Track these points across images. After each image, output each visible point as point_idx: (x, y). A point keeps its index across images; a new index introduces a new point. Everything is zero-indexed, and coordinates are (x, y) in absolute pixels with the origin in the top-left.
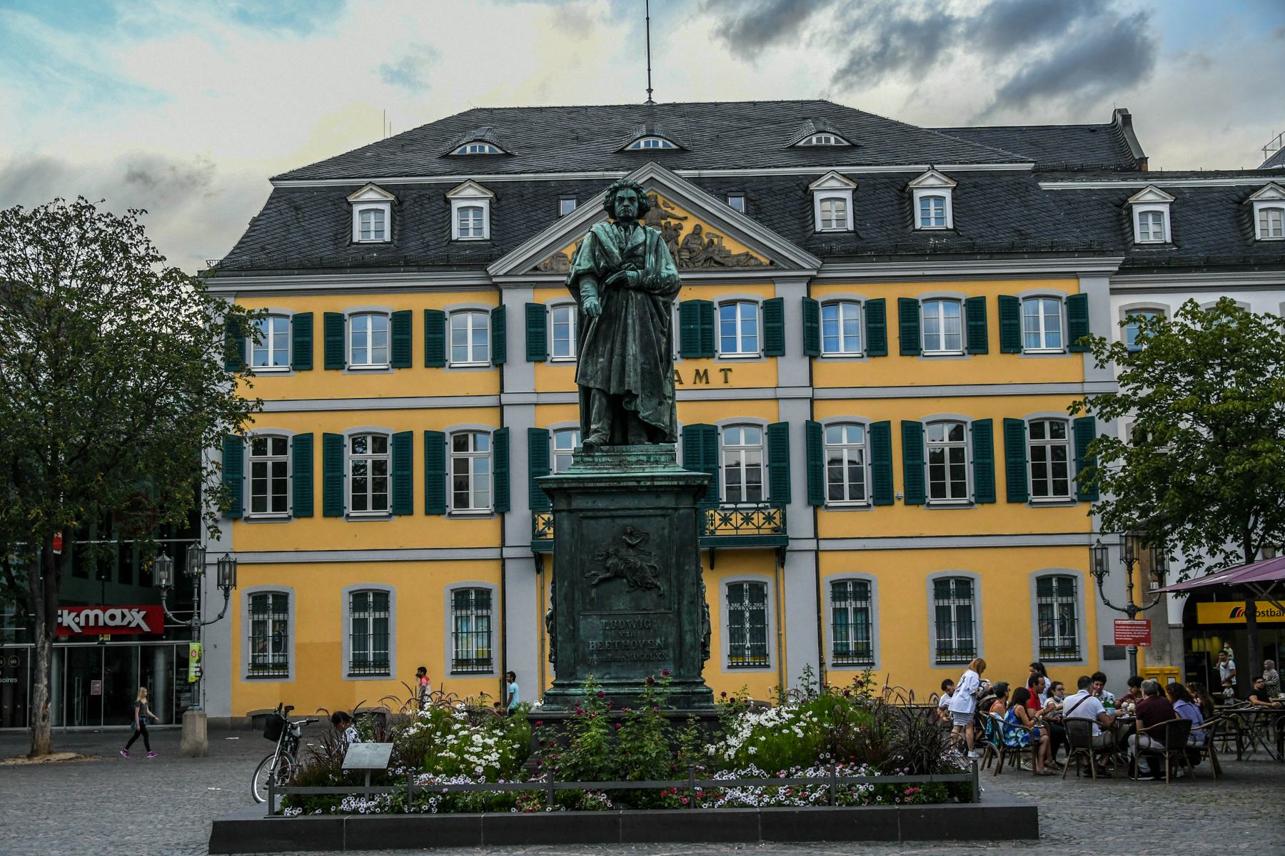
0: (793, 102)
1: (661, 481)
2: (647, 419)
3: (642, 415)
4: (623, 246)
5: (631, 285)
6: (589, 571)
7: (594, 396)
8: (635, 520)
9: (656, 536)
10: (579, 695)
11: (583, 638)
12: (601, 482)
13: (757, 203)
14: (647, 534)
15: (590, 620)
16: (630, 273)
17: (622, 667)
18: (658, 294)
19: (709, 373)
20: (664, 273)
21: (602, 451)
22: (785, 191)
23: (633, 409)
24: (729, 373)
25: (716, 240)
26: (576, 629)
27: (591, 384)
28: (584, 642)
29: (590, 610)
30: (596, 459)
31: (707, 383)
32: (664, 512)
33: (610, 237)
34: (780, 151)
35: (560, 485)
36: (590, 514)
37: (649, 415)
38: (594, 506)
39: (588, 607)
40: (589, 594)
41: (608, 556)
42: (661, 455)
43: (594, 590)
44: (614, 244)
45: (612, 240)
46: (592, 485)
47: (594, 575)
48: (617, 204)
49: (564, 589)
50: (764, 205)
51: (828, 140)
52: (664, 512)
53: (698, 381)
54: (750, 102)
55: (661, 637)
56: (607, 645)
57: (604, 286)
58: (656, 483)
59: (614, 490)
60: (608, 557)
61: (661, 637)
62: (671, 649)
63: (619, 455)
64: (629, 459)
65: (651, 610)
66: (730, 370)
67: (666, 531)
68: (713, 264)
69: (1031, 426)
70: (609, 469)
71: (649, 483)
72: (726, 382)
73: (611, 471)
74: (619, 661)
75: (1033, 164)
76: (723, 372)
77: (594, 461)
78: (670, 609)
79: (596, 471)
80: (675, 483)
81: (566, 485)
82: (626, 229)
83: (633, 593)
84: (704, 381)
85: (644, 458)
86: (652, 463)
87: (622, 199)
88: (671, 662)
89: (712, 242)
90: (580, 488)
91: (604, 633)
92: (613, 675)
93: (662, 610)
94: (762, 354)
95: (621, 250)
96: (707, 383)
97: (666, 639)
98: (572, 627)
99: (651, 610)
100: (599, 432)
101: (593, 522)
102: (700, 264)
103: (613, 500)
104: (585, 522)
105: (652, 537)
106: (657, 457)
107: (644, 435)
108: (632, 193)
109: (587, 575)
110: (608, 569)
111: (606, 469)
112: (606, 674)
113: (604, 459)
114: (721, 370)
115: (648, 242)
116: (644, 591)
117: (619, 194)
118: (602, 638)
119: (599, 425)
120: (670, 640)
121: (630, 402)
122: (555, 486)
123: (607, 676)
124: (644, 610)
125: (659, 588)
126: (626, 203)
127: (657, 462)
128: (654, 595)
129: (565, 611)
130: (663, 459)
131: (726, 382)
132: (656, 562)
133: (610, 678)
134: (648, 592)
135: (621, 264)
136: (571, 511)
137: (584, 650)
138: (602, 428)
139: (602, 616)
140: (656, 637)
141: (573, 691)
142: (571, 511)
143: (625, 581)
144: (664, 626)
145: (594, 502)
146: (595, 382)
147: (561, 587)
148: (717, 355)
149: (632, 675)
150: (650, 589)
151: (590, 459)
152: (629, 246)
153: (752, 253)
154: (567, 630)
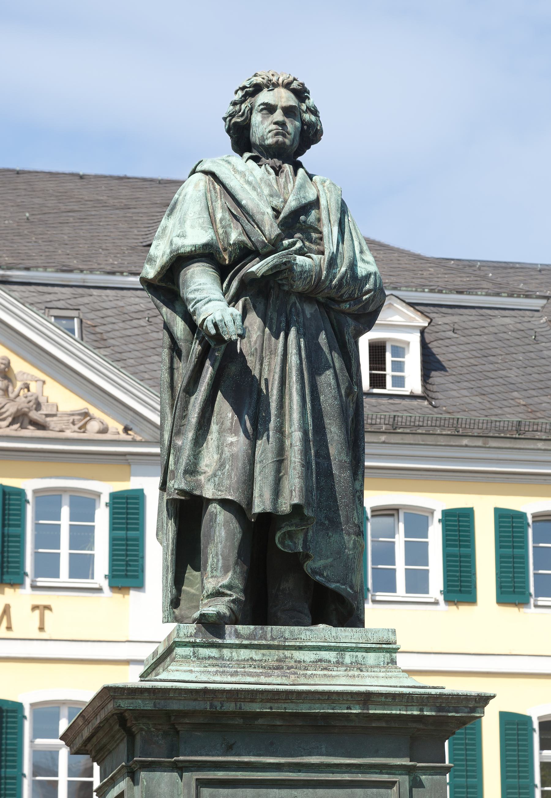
0: (145, 180)
2: (321, 575)
3: (309, 566)
4: (277, 202)
5: (299, 286)
7: (214, 517)
12: (253, 701)
13: (98, 330)
16: (300, 259)
18: (343, 312)
19: (13, 611)
20: (362, 270)
21: (238, 635)
22: (145, 314)
24: (47, 612)
25: (34, 387)
27: (208, 492)
30: (226, 652)
31: (9, 628)
33: (249, 183)
34: (133, 248)
35: (162, 704)
36: (221, 775)
37: (325, 567)
42: (367, 650)
44: (260, 195)
45: (254, 189)
46: (230, 707)
48: (256, 118)
50: (110, 335)
54: (73, 175)
57: (235, 284)
59: (278, 723)
63: (278, 648)
64: (298, 655)
66: (48, 608)
69: (541, 724)
70: (258, 675)
72: (41, 629)
73: (263, 679)
75: (544, 302)
76: (37, 612)
77: (222, 658)
79: (230, 679)
81: (175, 706)
82: (278, 171)
85: (331, 656)
86: (349, 667)
87: (270, 109)
89: (28, 387)
90: (203, 712)
95: (277, 212)
96: (9, 628)
100: (223, 595)
102: (6, 423)
103: (272, 744)
106: (359, 654)
107: (307, 611)
108: (290, 100)
111: (250, 675)
113: (244, 654)
114: (35, 608)
115: (323, 202)
117: (264, 97)
119: (226, 581)
121: (290, 535)
122: (148, 706)
126: (278, 116)
127: (360, 667)
130: (371, 658)
131: (41, 629)
135: (279, 238)
138: (230, 587)
146: (217, 487)
151: (213, 652)
152: (292, 203)
153: (93, 411)
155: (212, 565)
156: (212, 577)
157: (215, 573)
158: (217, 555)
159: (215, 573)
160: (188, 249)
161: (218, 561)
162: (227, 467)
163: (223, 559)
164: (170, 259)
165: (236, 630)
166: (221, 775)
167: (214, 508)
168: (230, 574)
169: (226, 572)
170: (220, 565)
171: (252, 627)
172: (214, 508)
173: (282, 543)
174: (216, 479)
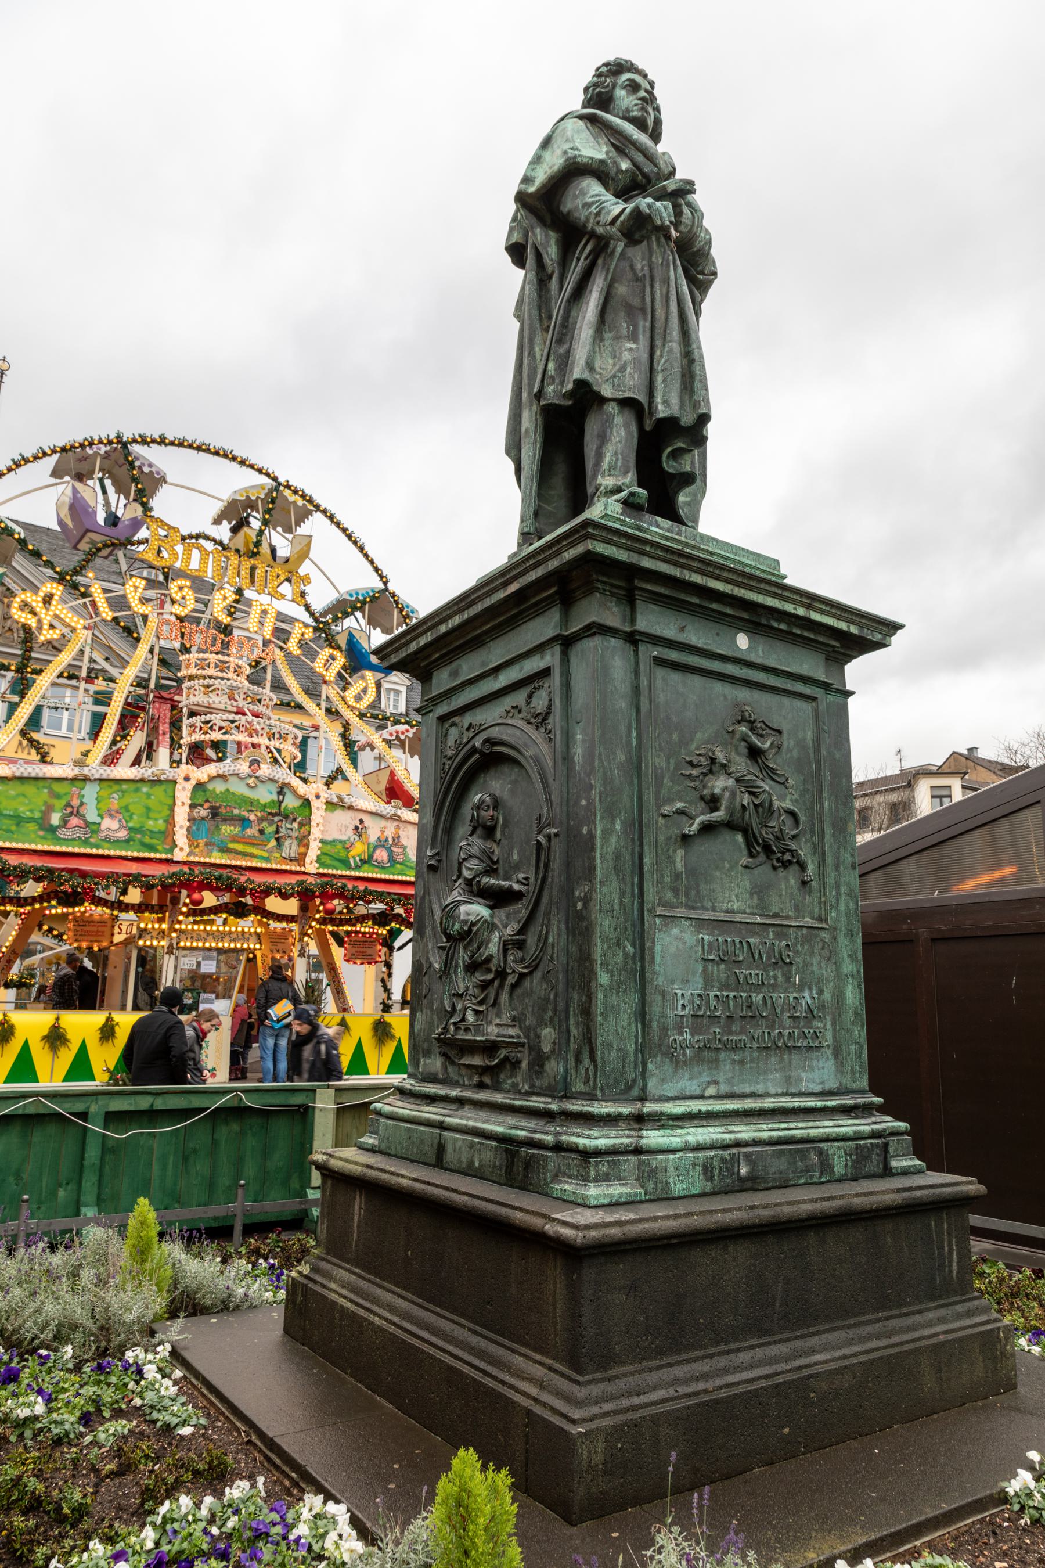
1: (822, 612)
6: (670, 801)
8: (757, 695)
9: (792, 743)
10: (674, 1151)
11: (660, 981)
14: (780, 732)
15: (675, 931)
17: (741, 1062)
23: (688, 469)
26: (642, 951)
28: (663, 994)
29: (672, 906)
32: (807, 690)
36: (674, 655)
38: (681, 638)
39: (669, 896)
40: (671, 860)
41: (714, 766)
43: (680, 853)
47: (681, 812)
49: (613, 840)
51: (156, 575)
52: (807, 690)
53: (20, 750)
55: (810, 988)
56: (713, 1003)
58: (815, 616)
60: (711, 771)
61: (810, 988)
62: (828, 1018)
65: (787, 917)
66: (53, 746)
67: (809, 735)
68: (50, 648)
71: (801, 612)
74: (735, 1049)
78: (820, 919)
80: (843, 626)
83: (756, 871)
84: (26, 751)
88: (829, 1052)
91: (704, 971)
92: (724, 1088)
93: (807, 921)
94: (87, 737)
97: (821, 992)
98: (630, 948)
99: (787, 917)
101: (675, 677)
103: (718, 634)
104: (660, 673)
105: (785, 743)
109: (666, 810)
110: (713, 802)
112: (709, 1083)
116: (775, 868)
118: (699, 981)
120: (827, 996)
121: (676, 454)
123: (711, 1091)
124: (776, 916)
125: (802, 866)
128: (792, 882)
129: (616, 907)
132: (795, 802)
133: (718, 1097)
134: (781, 873)
136: (633, 639)
137: (663, 1015)
139: (700, 923)
140: (801, 989)
141: (654, 1137)
142: (633, 639)
143: (739, 838)
144: (815, 961)
145: (682, 629)
147: (607, 833)
148: (42, 730)
149: (760, 1088)
150: (786, 865)
154: (620, 958)
155: (609, 463)
156: (609, 475)
157: (613, 472)
158: (616, 454)
159: (613, 472)
160: (585, 160)
161: (617, 460)
162: (629, 369)
163: (623, 459)
164: (564, 168)
165: (656, 521)
166: (674, 655)
167: (612, 408)
168: (630, 475)
169: (626, 473)
170: (619, 464)
171: (670, 522)
172: (612, 408)
173: (667, 463)
174: (616, 381)
